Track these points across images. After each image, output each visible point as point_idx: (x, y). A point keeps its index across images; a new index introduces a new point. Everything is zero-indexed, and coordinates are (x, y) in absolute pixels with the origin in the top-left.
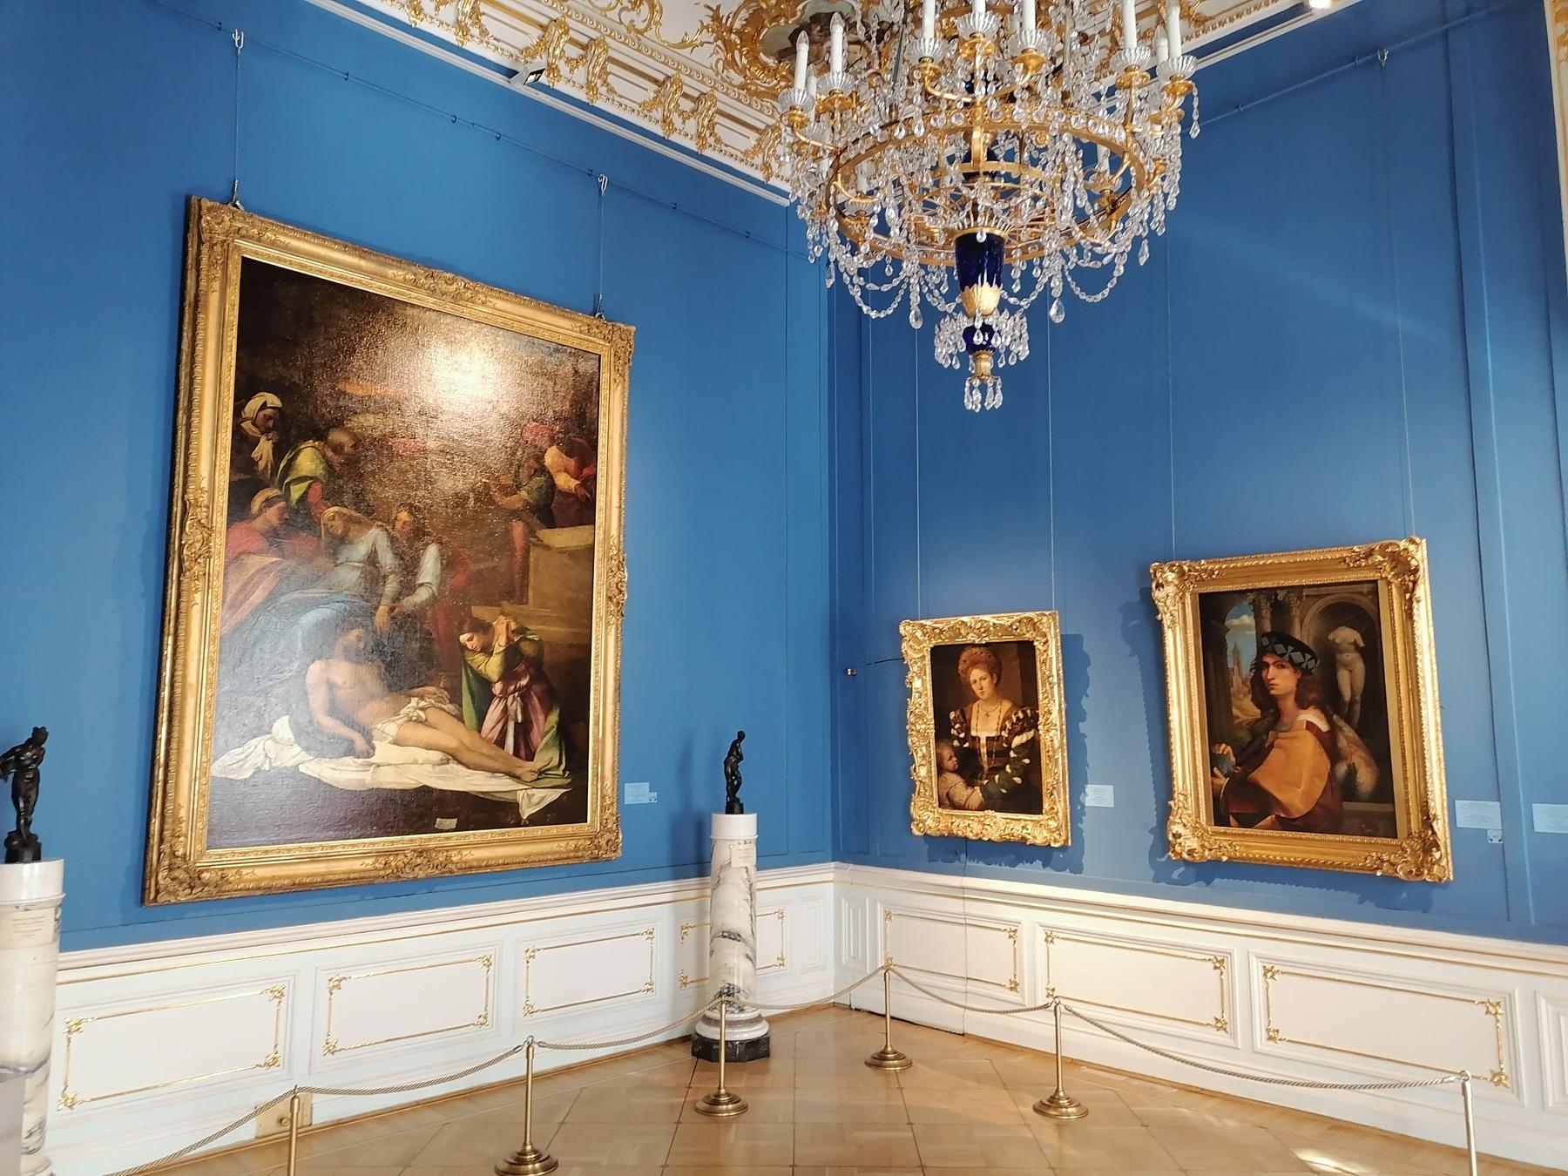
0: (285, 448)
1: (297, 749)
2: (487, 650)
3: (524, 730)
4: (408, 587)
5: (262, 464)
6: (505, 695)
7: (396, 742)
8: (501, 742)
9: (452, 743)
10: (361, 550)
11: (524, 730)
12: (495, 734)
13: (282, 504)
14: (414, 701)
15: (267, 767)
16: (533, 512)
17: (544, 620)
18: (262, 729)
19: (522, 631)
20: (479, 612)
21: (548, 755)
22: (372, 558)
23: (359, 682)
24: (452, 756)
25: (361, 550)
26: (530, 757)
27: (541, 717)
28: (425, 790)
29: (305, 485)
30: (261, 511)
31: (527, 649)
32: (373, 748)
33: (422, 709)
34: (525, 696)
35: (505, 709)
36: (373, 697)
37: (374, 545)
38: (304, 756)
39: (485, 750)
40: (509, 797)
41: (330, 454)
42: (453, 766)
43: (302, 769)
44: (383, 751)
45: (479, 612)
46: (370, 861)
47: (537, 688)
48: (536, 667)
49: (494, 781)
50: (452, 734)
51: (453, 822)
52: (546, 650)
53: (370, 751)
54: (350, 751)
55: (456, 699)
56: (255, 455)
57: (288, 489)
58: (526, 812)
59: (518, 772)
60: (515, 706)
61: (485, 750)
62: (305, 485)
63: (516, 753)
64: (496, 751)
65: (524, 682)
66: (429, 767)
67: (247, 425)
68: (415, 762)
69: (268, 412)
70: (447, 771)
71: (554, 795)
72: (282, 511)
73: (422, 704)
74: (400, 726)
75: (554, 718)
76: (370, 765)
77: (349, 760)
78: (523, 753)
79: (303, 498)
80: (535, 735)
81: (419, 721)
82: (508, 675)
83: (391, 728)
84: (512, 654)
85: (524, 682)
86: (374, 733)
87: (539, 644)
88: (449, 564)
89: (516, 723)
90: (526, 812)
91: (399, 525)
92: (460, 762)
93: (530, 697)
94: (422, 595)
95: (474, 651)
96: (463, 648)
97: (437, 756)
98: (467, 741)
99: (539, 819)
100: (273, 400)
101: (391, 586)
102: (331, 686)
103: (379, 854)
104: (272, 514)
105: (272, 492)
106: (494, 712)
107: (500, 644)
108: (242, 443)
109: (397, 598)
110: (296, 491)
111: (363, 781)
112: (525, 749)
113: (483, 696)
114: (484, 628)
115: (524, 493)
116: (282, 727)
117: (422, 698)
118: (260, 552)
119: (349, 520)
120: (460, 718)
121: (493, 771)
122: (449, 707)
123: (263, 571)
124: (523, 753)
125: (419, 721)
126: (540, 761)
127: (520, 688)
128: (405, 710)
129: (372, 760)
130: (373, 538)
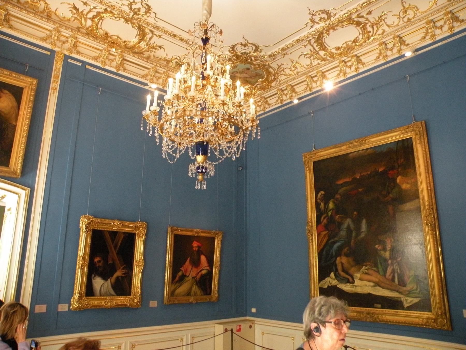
0: (326, 203)
1: (336, 281)
2: (384, 249)
7: (360, 279)
8: (393, 280)
9: (377, 280)
10: (345, 226)
12: (391, 277)
13: (327, 218)
14: (364, 268)
15: (330, 285)
18: (329, 275)
22: (348, 228)
24: (377, 284)
25: (345, 226)
28: (370, 295)
32: (354, 281)
33: (366, 269)
36: (352, 266)
38: (338, 283)
41: (336, 202)
43: (338, 286)
44: (357, 282)
46: (355, 314)
49: (392, 293)
50: (375, 277)
51: (380, 306)
53: (353, 282)
54: (348, 282)
55: (376, 266)
56: (321, 207)
57: (328, 214)
58: (406, 305)
59: (401, 290)
61: (388, 283)
66: (370, 287)
67: (318, 201)
68: (366, 286)
71: (416, 300)
73: (366, 268)
76: (354, 286)
77: (348, 284)
79: (332, 214)
83: (358, 275)
86: (354, 277)
90: (406, 305)
91: (354, 216)
92: (380, 286)
94: (363, 235)
95: (380, 250)
97: (372, 284)
98: (381, 279)
100: (322, 192)
102: (342, 264)
103: (358, 312)
104: (325, 220)
108: (318, 205)
109: (356, 236)
110: (330, 213)
111: (352, 290)
115: (391, 195)
116: (332, 275)
117: (366, 266)
118: (324, 231)
120: (378, 272)
122: (375, 269)
123: (325, 235)
128: (361, 270)
129: (354, 284)
130: (348, 222)
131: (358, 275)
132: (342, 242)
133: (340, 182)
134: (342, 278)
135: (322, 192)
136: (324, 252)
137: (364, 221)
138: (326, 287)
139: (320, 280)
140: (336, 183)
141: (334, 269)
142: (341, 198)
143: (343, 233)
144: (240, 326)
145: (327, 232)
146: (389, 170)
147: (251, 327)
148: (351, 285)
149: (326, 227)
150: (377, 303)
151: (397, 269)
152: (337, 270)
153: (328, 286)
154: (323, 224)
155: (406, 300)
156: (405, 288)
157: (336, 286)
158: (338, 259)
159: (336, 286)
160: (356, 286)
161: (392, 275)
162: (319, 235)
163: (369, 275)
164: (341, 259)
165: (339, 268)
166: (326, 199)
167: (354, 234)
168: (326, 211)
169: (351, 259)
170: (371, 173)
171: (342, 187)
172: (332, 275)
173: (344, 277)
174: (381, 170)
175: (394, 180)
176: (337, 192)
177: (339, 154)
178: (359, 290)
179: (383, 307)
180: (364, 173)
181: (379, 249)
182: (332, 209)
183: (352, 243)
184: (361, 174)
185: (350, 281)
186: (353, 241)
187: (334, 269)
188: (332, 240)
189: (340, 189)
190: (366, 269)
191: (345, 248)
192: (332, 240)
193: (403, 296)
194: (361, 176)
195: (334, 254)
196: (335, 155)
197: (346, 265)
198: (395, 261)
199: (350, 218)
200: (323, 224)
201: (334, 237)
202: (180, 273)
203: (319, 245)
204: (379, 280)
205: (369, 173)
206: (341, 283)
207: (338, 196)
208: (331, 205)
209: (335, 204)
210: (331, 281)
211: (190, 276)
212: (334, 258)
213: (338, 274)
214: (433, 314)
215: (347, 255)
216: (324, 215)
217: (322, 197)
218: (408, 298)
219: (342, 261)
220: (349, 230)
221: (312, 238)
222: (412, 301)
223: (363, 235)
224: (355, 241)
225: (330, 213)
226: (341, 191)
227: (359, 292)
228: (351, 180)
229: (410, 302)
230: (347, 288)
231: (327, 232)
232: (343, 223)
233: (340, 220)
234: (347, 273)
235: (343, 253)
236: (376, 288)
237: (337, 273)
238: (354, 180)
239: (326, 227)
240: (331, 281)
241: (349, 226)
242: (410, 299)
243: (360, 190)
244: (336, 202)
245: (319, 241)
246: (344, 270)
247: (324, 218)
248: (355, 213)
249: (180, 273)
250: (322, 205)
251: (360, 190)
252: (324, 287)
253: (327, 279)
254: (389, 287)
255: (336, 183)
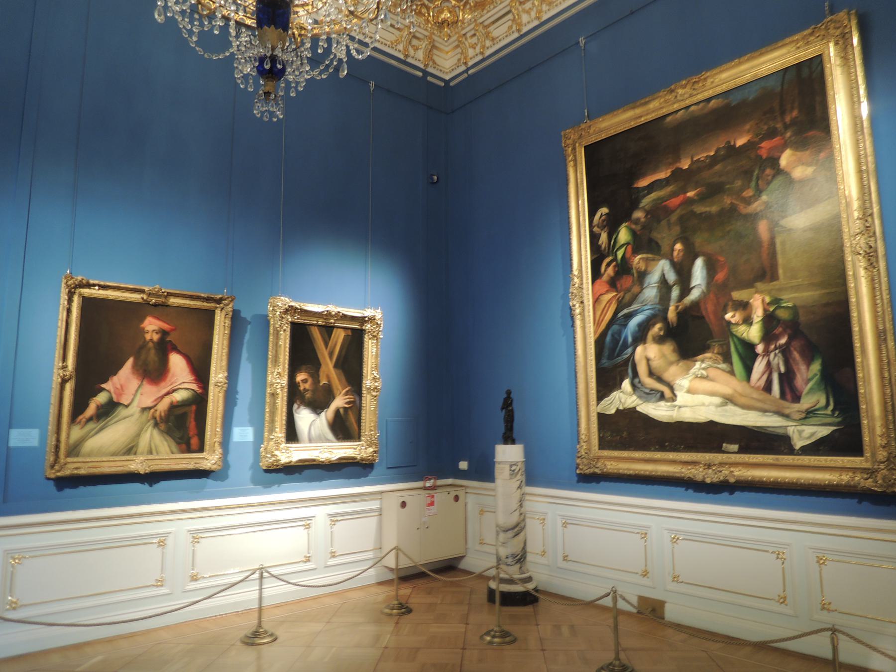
0: (613, 232)
1: (634, 397)
2: (748, 321)
3: (787, 379)
4: (686, 290)
5: (603, 246)
6: (767, 352)
7: (689, 391)
8: (768, 388)
9: (727, 391)
11: (787, 379)
13: (614, 263)
14: (698, 365)
15: (621, 408)
16: (757, 214)
17: (797, 288)
18: (617, 386)
19: (776, 301)
20: (737, 295)
21: (813, 398)
22: (663, 281)
23: (663, 356)
24: (729, 400)
26: (797, 398)
27: (803, 367)
28: (712, 423)
29: (623, 249)
30: (605, 271)
31: (783, 314)
32: (675, 396)
33: (704, 369)
34: (785, 351)
35: (769, 364)
36: (671, 364)
37: (663, 271)
38: (638, 401)
39: (755, 395)
40: (781, 431)
41: (633, 226)
42: (730, 407)
43: (638, 409)
44: (682, 398)
45: (737, 295)
47: (796, 344)
48: (794, 328)
51: (735, 447)
52: (801, 312)
53: (674, 398)
54: (662, 397)
56: (600, 243)
58: (798, 444)
59: (787, 411)
60: (778, 361)
62: (623, 249)
63: (783, 395)
64: (764, 396)
65: (783, 341)
66: (713, 408)
67: (596, 229)
68: (703, 405)
69: (603, 217)
70: (726, 411)
72: (615, 266)
73: (704, 365)
74: (691, 381)
75: (816, 367)
77: (662, 403)
78: (789, 396)
80: (799, 381)
81: (702, 377)
82: (768, 336)
84: (770, 320)
85: (783, 341)
86: (676, 387)
87: (794, 309)
88: (711, 268)
89: (780, 375)
90: (798, 444)
91: (675, 253)
92: (736, 404)
93: (790, 352)
94: (695, 295)
95: (737, 324)
96: (729, 323)
99: (817, 448)
100: (604, 210)
101: (675, 293)
102: (648, 360)
105: (610, 258)
106: (759, 366)
107: (758, 314)
108: (594, 238)
110: (620, 254)
111: (671, 416)
112: (790, 391)
113: (748, 353)
114: (744, 306)
117: (703, 361)
118: (607, 292)
119: (647, 260)
120: (732, 373)
121: (765, 411)
122: (723, 366)
124: (789, 396)
125: (702, 377)
126: (807, 402)
127: (781, 346)
128: (692, 371)
129: (676, 403)
130: (662, 268)
131: (683, 383)
132: (648, 313)
133: (643, 183)
134: (647, 391)
135: (604, 210)
136: (608, 338)
137: (699, 263)
138: (613, 411)
139: (600, 398)
140: (635, 186)
141: (630, 371)
142: (646, 216)
143: (651, 293)
144: (433, 497)
145: (614, 294)
146: (762, 140)
147: (457, 498)
148: (669, 404)
149: (613, 284)
150: (731, 442)
151: (778, 364)
152: (635, 374)
153: (618, 411)
154: (605, 278)
155: (800, 432)
156: (796, 406)
157: (635, 408)
158: (639, 349)
159: (635, 408)
160: (680, 407)
161: (765, 377)
162: (596, 301)
163: (712, 380)
164: (645, 349)
165: (642, 369)
166: (612, 226)
167: (675, 293)
168: (612, 249)
169: (668, 349)
170: (716, 152)
171: (649, 193)
172: (626, 384)
173: (652, 390)
174: (740, 142)
175: (774, 162)
176: (635, 205)
177: (643, 120)
178: (688, 416)
179: (742, 450)
180: (701, 156)
181: (733, 321)
182: (628, 244)
183: (672, 315)
184: (692, 158)
185: (665, 394)
186: (672, 308)
187: (630, 371)
188: (625, 311)
189: (644, 196)
190: (704, 369)
191: (654, 324)
192: (625, 311)
193: (791, 423)
194: (693, 163)
195: (630, 340)
196: (633, 124)
197: (656, 363)
198: (773, 347)
199: (667, 258)
200: (605, 278)
201: (630, 304)
202: (101, 398)
203: (597, 323)
204: (735, 391)
205: (712, 154)
206: (647, 401)
207: (638, 214)
208: (623, 235)
209: (633, 233)
210: (625, 397)
211: (135, 403)
212: (630, 350)
213: (640, 382)
214: (867, 461)
215: (660, 340)
216: (610, 258)
217: (603, 221)
218: (803, 427)
219: (650, 353)
220: (664, 286)
221: (583, 310)
222: (813, 434)
223: (695, 295)
224: (677, 307)
225: (620, 254)
226: (646, 201)
227: (687, 420)
228: (668, 174)
229: (809, 438)
230: (659, 411)
231: (614, 294)
232: (649, 274)
233: (642, 266)
234: (660, 379)
235: (650, 336)
236: (726, 408)
237: (636, 381)
238: (678, 174)
239: (613, 284)
240: (625, 397)
241: (663, 276)
242: (808, 430)
243: (690, 194)
244: (633, 226)
245: (597, 318)
246: (651, 374)
247: (608, 265)
248: (678, 246)
249: (101, 398)
250: (604, 237)
251: (690, 194)
252: (608, 413)
253: (615, 395)
254: (759, 405)
255: (635, 186)
